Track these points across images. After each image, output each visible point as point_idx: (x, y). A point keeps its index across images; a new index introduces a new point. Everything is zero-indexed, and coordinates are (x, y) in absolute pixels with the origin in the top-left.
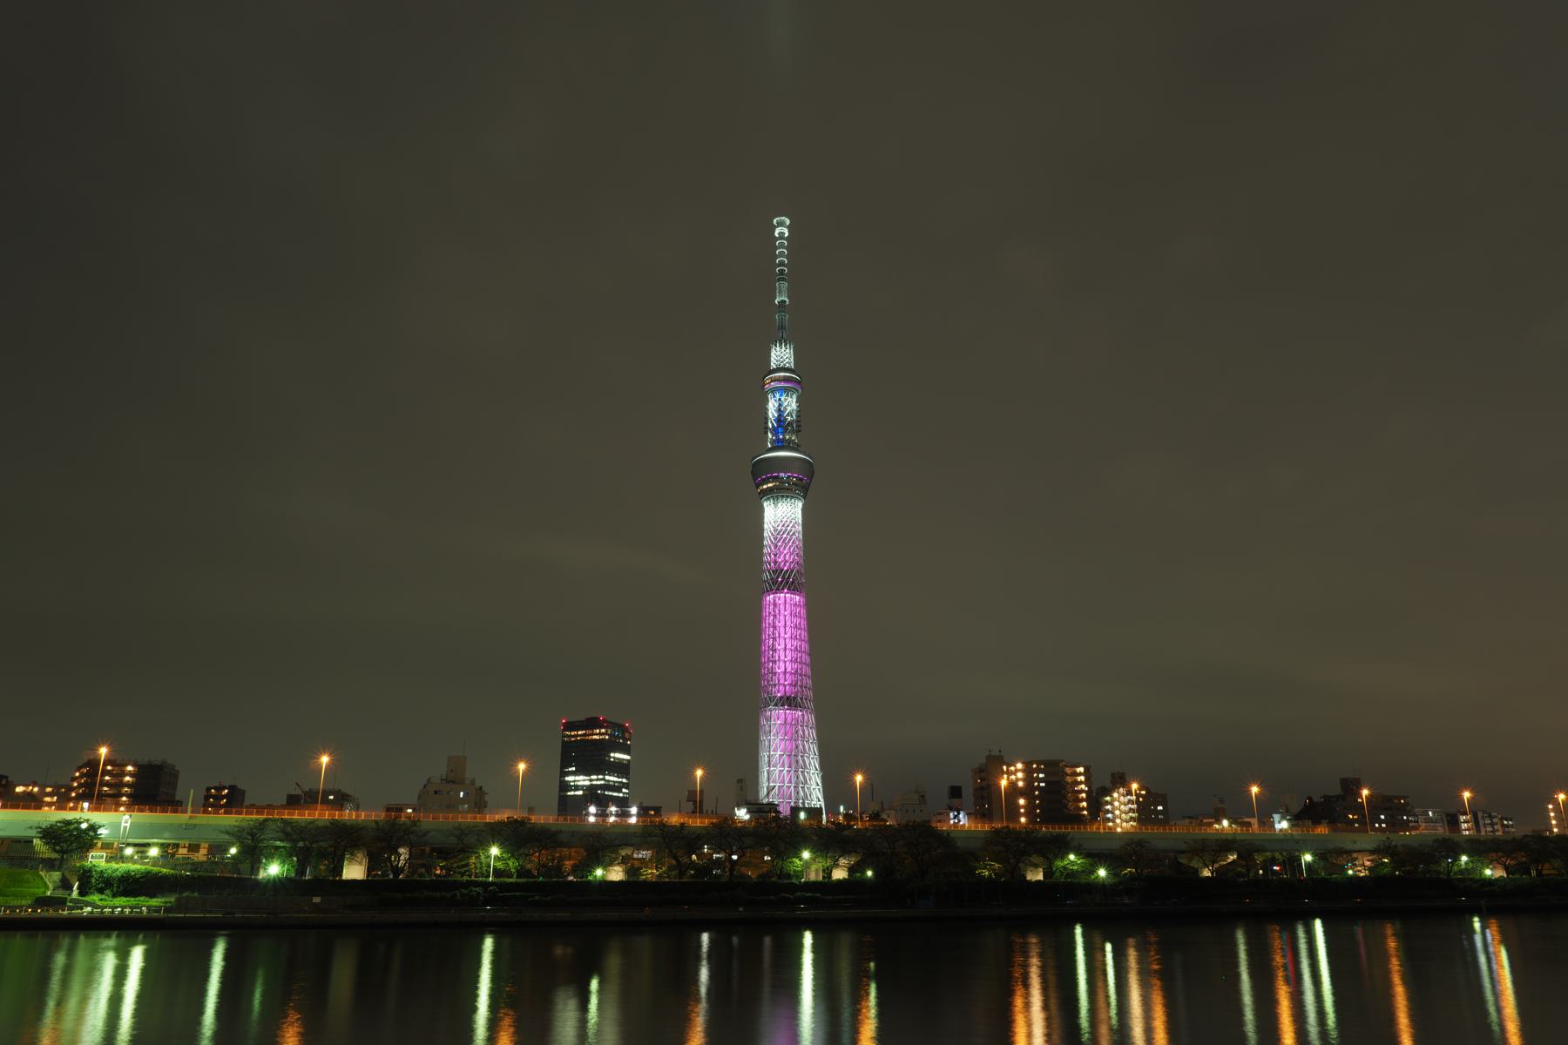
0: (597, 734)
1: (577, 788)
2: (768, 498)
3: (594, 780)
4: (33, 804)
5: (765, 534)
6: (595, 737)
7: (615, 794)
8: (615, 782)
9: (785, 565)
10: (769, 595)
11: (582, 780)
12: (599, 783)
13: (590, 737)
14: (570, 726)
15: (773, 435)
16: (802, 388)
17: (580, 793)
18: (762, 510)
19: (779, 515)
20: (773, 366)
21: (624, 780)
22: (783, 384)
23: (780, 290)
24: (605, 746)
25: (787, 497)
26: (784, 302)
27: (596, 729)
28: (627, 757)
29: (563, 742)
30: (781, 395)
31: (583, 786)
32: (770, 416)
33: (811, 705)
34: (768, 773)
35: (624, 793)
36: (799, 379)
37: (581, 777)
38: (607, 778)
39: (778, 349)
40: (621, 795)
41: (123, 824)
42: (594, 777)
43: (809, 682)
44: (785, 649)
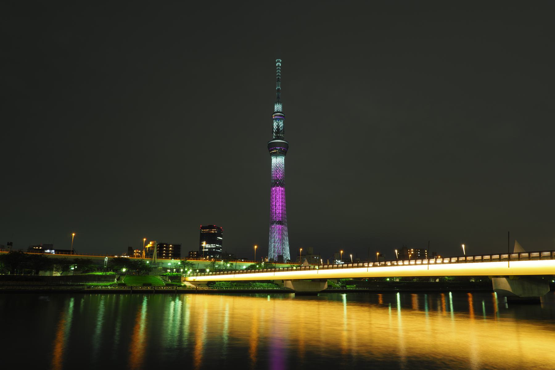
0: (213, 231)
1: (205, 248)
2: (274, 156)
3: (212, 246)
4: (60, 252)
5: (272, 167)
6: (212, 232)
7: (218, 251)
8: (219, 247)
9: (279, 178)
10: (274, 187)
11: (208, 246)
12: (214, 247)
13: (211, 232)
14: (203, 228)
15: (275, 134)
16: (285, 119)
17: (207, 250)
18: (271, 159)
19: (278, 161)
20: (276, 110)
21: (221, 246)
22: (279, 117)
23: (278, 85)
24: (215, 235)
25: (281, 155)
26: (279, 89)
27: (213, 229)
28: (221, 239)
29: (201, 233)
30: (278, 121)
31: (208, 248)
32: (274, 127)
33: (287, 224)
34: (274, 245)
35: (221, 250)
36: (283, 116)
37: (208, 245)
38: (216, 245)
39: (277, 105)
40: (220, 251)
41: (105, 260)
42: (212, 245)
43: (286, 216)
44: (279, 206)
